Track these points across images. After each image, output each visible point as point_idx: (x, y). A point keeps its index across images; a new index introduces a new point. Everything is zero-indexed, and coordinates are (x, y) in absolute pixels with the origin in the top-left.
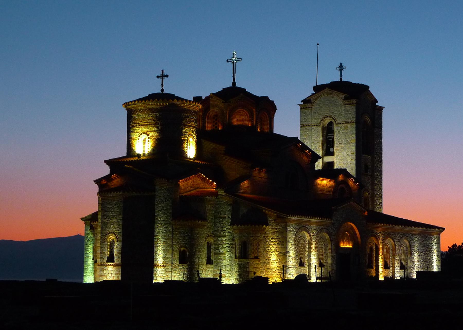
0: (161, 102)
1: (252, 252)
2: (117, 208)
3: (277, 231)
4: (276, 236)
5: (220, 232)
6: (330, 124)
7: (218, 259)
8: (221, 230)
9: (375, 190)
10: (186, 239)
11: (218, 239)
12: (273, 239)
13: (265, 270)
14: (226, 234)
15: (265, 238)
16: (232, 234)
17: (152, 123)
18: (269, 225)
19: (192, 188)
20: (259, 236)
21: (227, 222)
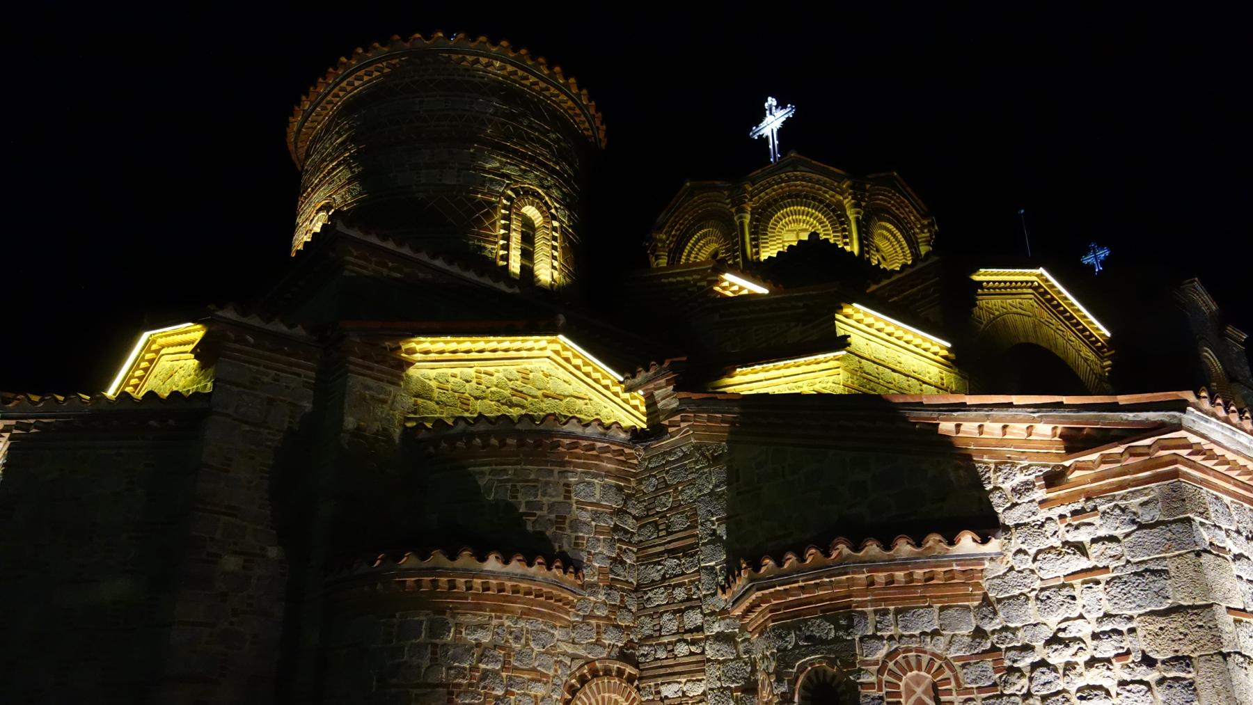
3: (1095, 568)
5: (670, 648)
11: (658, 692)
12: (1066, 643)
14: (703, 653)
16: (741, 648)
18: (1007, 529)
20: (935, 633)
21: (706, 568)
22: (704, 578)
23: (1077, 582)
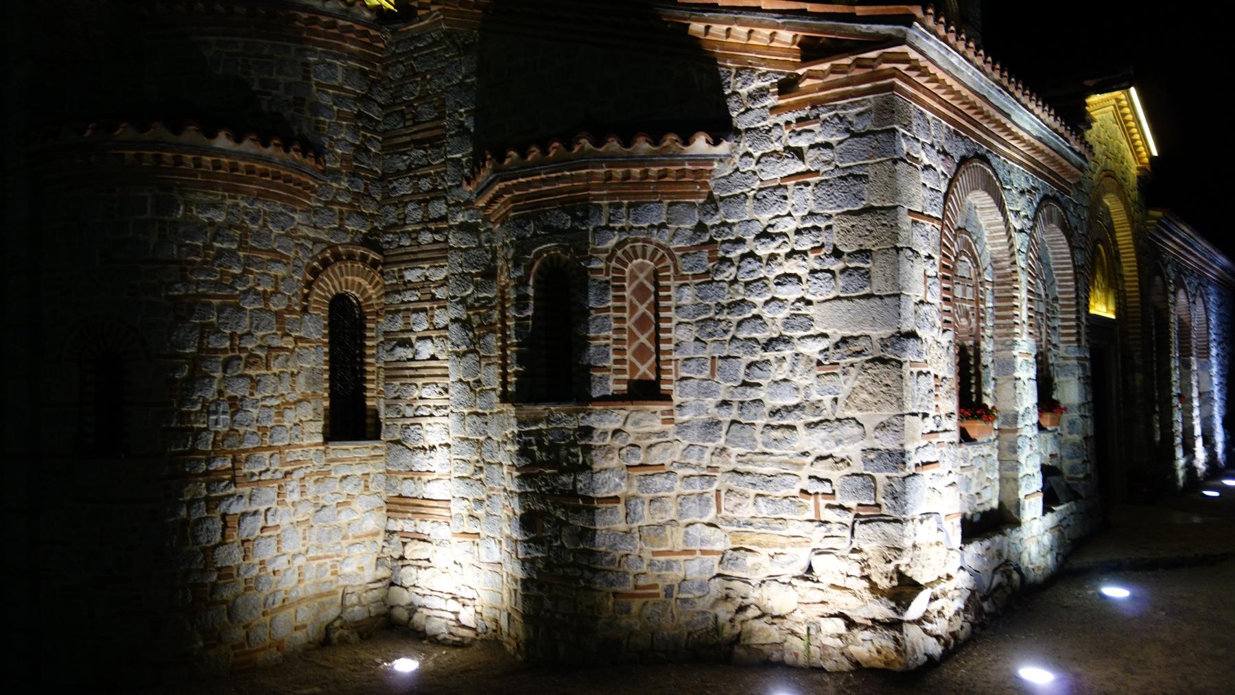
3: (808, 173)
4: (801, 214)
7: (410, 405)
8: (422, 222)
11: (402, 277)
12: (772, 237)
13: (716, 485)
14: (446, 241)
16: (483, 237)
18: (738, 132)
20: (663, 226)
21: (452, 160)
22: (450, 169)
23: (790, 183)
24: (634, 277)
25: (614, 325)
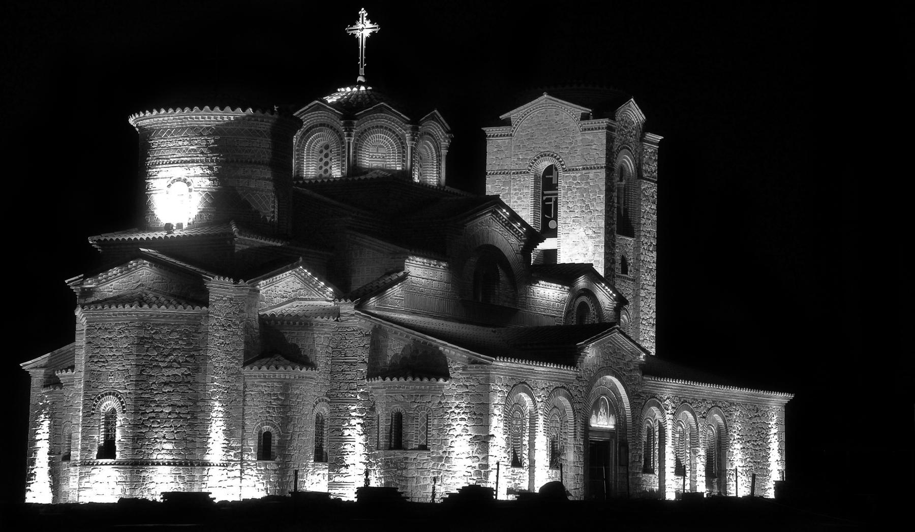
0: (217, 114)
1: (412, 434)
2: (124, 340)
6: (550, 170)
9: (642, 311)
10: (274, 408)
12: (459, 408)
13: (441, 474)
14: (356, 397)
15: (443, 407)
17: (198, 158)
18: (451, 378)
19: (284, 300)
20: (430, 402)
24: (421, 416)
25: (415, 429)
